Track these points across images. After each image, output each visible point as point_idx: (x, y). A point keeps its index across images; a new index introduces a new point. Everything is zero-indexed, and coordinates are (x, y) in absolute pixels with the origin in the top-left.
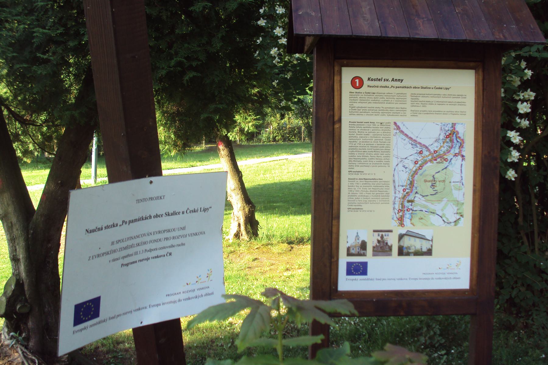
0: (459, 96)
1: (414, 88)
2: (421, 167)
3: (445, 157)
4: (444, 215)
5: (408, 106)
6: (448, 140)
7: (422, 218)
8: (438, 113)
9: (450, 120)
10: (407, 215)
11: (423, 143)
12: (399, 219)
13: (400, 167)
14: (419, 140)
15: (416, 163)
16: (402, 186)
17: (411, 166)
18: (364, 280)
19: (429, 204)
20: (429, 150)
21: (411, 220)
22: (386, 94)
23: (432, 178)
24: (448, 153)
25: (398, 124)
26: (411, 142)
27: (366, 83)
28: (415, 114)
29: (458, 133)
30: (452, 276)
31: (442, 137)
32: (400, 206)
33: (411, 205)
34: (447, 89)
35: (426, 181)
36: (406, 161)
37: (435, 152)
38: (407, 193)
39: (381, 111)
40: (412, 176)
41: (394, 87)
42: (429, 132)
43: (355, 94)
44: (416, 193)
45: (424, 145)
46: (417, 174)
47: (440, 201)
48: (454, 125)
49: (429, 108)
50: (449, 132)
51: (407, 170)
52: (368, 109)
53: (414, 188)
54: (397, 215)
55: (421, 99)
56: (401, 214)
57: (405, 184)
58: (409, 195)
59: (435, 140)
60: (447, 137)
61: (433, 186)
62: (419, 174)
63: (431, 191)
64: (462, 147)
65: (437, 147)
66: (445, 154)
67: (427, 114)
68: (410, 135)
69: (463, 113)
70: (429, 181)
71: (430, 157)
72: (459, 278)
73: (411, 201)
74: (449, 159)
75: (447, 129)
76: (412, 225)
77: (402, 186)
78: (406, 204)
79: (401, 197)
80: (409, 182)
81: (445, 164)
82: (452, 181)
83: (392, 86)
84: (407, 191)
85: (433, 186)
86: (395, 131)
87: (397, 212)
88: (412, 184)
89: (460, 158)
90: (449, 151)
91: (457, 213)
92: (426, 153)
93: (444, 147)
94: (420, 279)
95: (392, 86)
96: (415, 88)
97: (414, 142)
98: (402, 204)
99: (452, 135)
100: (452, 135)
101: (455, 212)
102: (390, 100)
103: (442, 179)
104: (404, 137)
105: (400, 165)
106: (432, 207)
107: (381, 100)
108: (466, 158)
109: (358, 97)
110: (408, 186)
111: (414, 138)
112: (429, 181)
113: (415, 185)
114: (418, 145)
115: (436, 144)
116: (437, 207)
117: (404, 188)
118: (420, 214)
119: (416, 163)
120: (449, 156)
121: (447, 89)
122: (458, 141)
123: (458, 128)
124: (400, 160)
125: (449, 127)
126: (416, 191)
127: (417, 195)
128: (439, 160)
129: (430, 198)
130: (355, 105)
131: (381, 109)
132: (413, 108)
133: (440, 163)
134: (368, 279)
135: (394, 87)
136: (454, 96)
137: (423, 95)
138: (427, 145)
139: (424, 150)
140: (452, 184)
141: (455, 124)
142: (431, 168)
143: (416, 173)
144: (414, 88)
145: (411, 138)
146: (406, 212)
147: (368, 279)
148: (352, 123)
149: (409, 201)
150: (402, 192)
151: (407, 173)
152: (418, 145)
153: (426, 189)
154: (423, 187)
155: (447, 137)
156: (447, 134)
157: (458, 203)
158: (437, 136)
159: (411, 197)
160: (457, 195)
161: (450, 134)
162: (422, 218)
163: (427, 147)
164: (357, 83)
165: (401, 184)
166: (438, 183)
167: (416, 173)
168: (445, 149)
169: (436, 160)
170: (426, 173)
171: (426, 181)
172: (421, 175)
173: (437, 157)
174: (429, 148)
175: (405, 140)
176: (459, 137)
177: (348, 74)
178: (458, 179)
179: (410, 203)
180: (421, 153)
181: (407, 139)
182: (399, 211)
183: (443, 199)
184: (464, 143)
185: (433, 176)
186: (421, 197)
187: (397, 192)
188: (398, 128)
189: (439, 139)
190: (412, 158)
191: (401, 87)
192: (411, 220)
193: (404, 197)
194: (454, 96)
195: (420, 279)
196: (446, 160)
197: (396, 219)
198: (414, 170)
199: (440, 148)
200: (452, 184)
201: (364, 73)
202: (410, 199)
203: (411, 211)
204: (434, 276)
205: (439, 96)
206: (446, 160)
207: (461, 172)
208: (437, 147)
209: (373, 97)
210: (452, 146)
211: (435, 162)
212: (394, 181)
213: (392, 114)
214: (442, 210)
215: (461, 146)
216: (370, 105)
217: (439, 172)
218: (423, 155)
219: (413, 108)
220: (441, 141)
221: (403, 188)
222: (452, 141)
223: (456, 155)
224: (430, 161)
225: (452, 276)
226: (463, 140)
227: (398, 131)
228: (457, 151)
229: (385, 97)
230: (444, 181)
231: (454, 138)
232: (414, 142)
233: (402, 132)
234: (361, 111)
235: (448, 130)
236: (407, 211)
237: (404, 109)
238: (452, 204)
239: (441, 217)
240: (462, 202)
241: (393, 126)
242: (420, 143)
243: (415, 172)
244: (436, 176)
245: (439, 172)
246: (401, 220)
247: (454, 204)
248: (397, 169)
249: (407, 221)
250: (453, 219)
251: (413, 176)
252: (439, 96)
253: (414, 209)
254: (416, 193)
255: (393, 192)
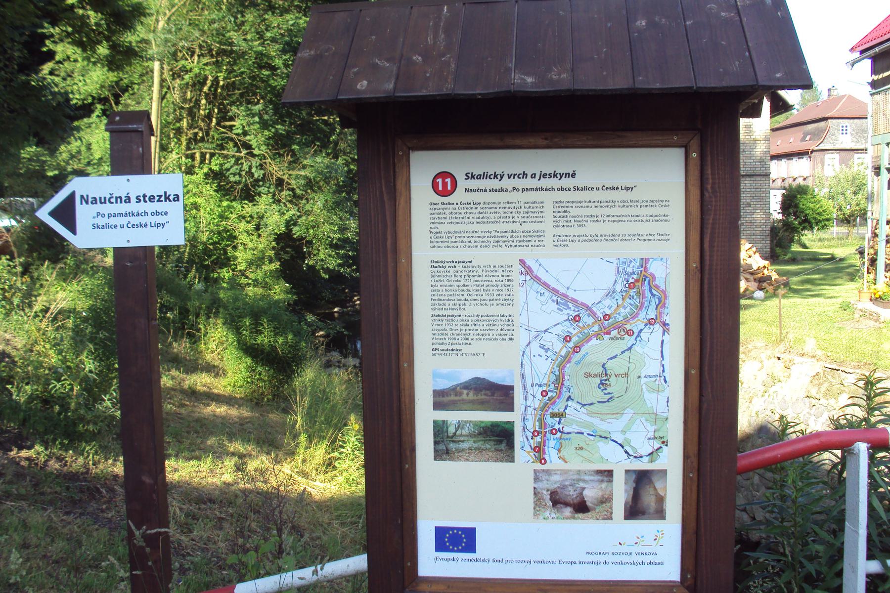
0: (653, 203)
1: (558, 189)
2: (577, 349)
3: (628, 327)
4: (628, 442)
5: (548, 227)
6: (632, 292)
7: (581, 448)
8: (611, 238)
9: (636, 251)
10: (552, 442)
11: (581, 298)
12: (534, 450)
13: (535, 348)
14: (571, 294)
15: (567, 339)
16: (540, 386)
17: (557, 345)
18: (468, 560)
19: (596, 421)
20: (593, 314)
21: (559, 451)
22: (502, 205)
23: (601, 370)
24: (633, 318)
25: (529, 262)
26: (555, 298)
27: (462, 183)
28: (561, 242)
29: (654, 278)
30: (647, 559)
31: (619, 288)
32: (537, 423)
33: (559, 423)
34: (627, 189)
35: (588, 375)
36: (547, 336)
37: (607, 317)
38: (549, 399)
39: (492, 239)
40: (559, 366)
41: (518, 190)
42: (591, 275)
43: (440, 206)
44: (569, 398)
45: (583, 304)
46: (569, 362)
47: (619, 414)
48: (644, 262)
49: (591, 228)
50: (635, 277)
51: (549, 354)
52: (466, 235)
53: (565, 389)
54: (532, 441)
55: (574, 211)
56: (538, 439)
57: (545, 381)
58: (554, 403)
59: (606, 292)
60: (630, 287)
61: (603, 385)
62: (573, 361)
63: (600, 395)
64: (664, 306)
65: (610, 307)
66: (626, 320)
67: (589, 241)
68: (553, 284)
69: (664, 238)
70: (595, 376)
71: (596, 328)
72: (661, 563)
73: (560, 415)
74: (636, 331)
75: (630, 270)
76: (561, 461)
77: (540, 386)
78: (549, 420)
79: (537, 406)
80: (553, 378)
81: (629, 340)
82: (643, 375)
83: (514, 189)
84: (550, 394)
85: (603, 385)
86: (523, 277)
87: (530, 435)
88: (559, 381)
89: (658, 328)
90: (637, 315)
91: (655, 438)
92: (587, 320)
93: (625, 308)
94: (580, 563)
95: (514, 189)
96: (562, 189)
97: (562, 299)
98: (540, 420)
99: (640, 282)
100: (640, 282)
101: (651, 435)
102: (511, 215)
103: (622, 371)
104: (541, 289)
105: (535, 345)
106: (603, 427)
107: (492, 216)
108: (671, 327)
109: (447, 212)
110: (552, 386)
111: (562, 290)
112: (595, 376)
113: (566, 383)
114: (571, 305)
115: (608, 302)
116: (614, 427)
117: (545, 388)
118: (577, 440)
119: (567, 339)
120: (636, 325)
121: (627, 189)
122: (653, 294)
123: (654, 268)
124: (533, 334)
125: (634, 267)
126: (567, 395)
127: (570, 403)
128: (614, 333)
129: (597, 408)
130: (441, 228)
131: (493, 234)
132: (559, 231)
133: (617, 339)
134: (477, 560)
135: (518, 190)
136: (644, 204)
137: (579, 204)
138: (590, 304)
139: (583, 313)
140: (643, 380)
141: (647, 260)
142: (598, 351)
143: (567, 359)
144: (558, 189)
145: (555, 291)
146: (548, 435)
147: (477, 560)
148: (436, 264)
149: (553, 415)
150: (539, 396)
151: (549, 360)
152: (571, 305)
153: (590, 391)
154: (583, 387)
155: (631, 286)
156: (631, 280)
157: (655, 418)
158: (608, 283)
159: (559, 407)
160: (654, 401)
161: (637, 281)
162: (581, 448)
163: (588, 308)
164: (444, 184)
165: (536, 381)
166: (613, 379)
167: (567, 359)
168: (628, 310)
169: (608, 333)
170: (588, 359)
171: (588, 375)
172: (578, 363)
173: (609, 326)
174: (594, 309)
175: (542, 294)
176: (657, 287)
177: (423, 168)
178: (655, 369)
179: (558, 419)
180: (577, 319)
181: (547, 294)
182: (535, 434)
183: (624, 410)
184: (666, 297)
185: (604, 365)
186: (578, 407)
187: (530, 398)
188: (528, 270)
189: (614, 292)
190: (559, 330)
191: (532, 189)
192: (559, 451)
193: (544, 408)
194: (644, 204)
195: (580, 563)
196: (630, 333)
197: (529, 449)
198: (563, 353)
199: (615, 310)
200: (643, 380)
201: (458, 162)
202: (556, 410)
203: (559, 434)
204: (610, 558)
205: (611, 203)
206: (630, 333)
207: (662, 356)
208: (610, 307)
209: (476, 211)
210: (643, 304)
211: (606, 337)
212: (523, 376)
213: (515, 244)
214: (624, 432)
215: (661, 304)
216: (470, 228)
217: (615, 357)
218: (581, 324)
219: (559, 231)
220: (618, 296)
221: (541, 389)
222: (641, 294)
223: (650, 322)
224: (597, 335)
225: (647, 559)
226: (664, 292)
227: (528, 278)
228: (652, 314)
229: (501, 211)
230: (626, 375)
231: (647, 288)
232: (562, 299)
233: (537, 279)
234: (454, 239)
235: (633, 273)
236: (552, 433)
237: (539, 234)
238: (643, 419)
239: (623, 447)
240: (665, 415)
241: (518, 268)
242: (574, 301)
243: (565, 357)
244: (610, 365)
245: (615, 357)
246: (539, 451)
247: (647, 420)
248: (528, 350)
249: (551, 454)
250: (646, 449)
251: (561, 366)
252: (611, 203)
253: (566, 430)
254: (569, 398)
255: (522, 397)
